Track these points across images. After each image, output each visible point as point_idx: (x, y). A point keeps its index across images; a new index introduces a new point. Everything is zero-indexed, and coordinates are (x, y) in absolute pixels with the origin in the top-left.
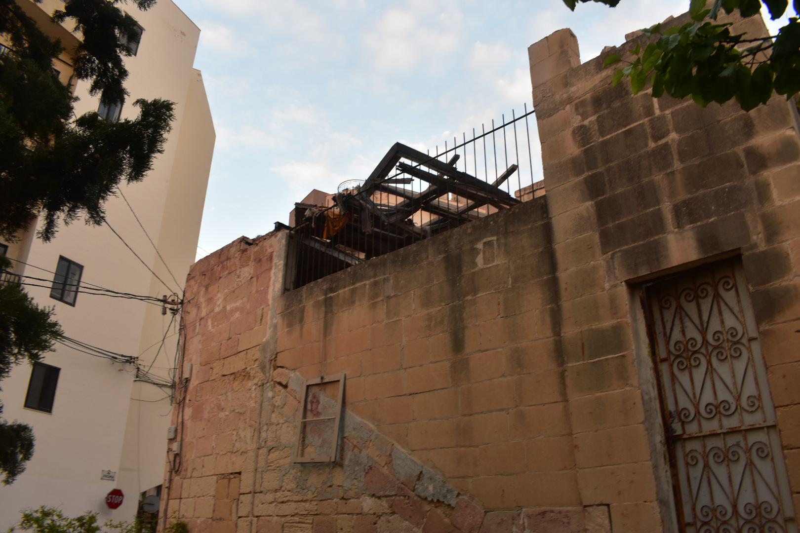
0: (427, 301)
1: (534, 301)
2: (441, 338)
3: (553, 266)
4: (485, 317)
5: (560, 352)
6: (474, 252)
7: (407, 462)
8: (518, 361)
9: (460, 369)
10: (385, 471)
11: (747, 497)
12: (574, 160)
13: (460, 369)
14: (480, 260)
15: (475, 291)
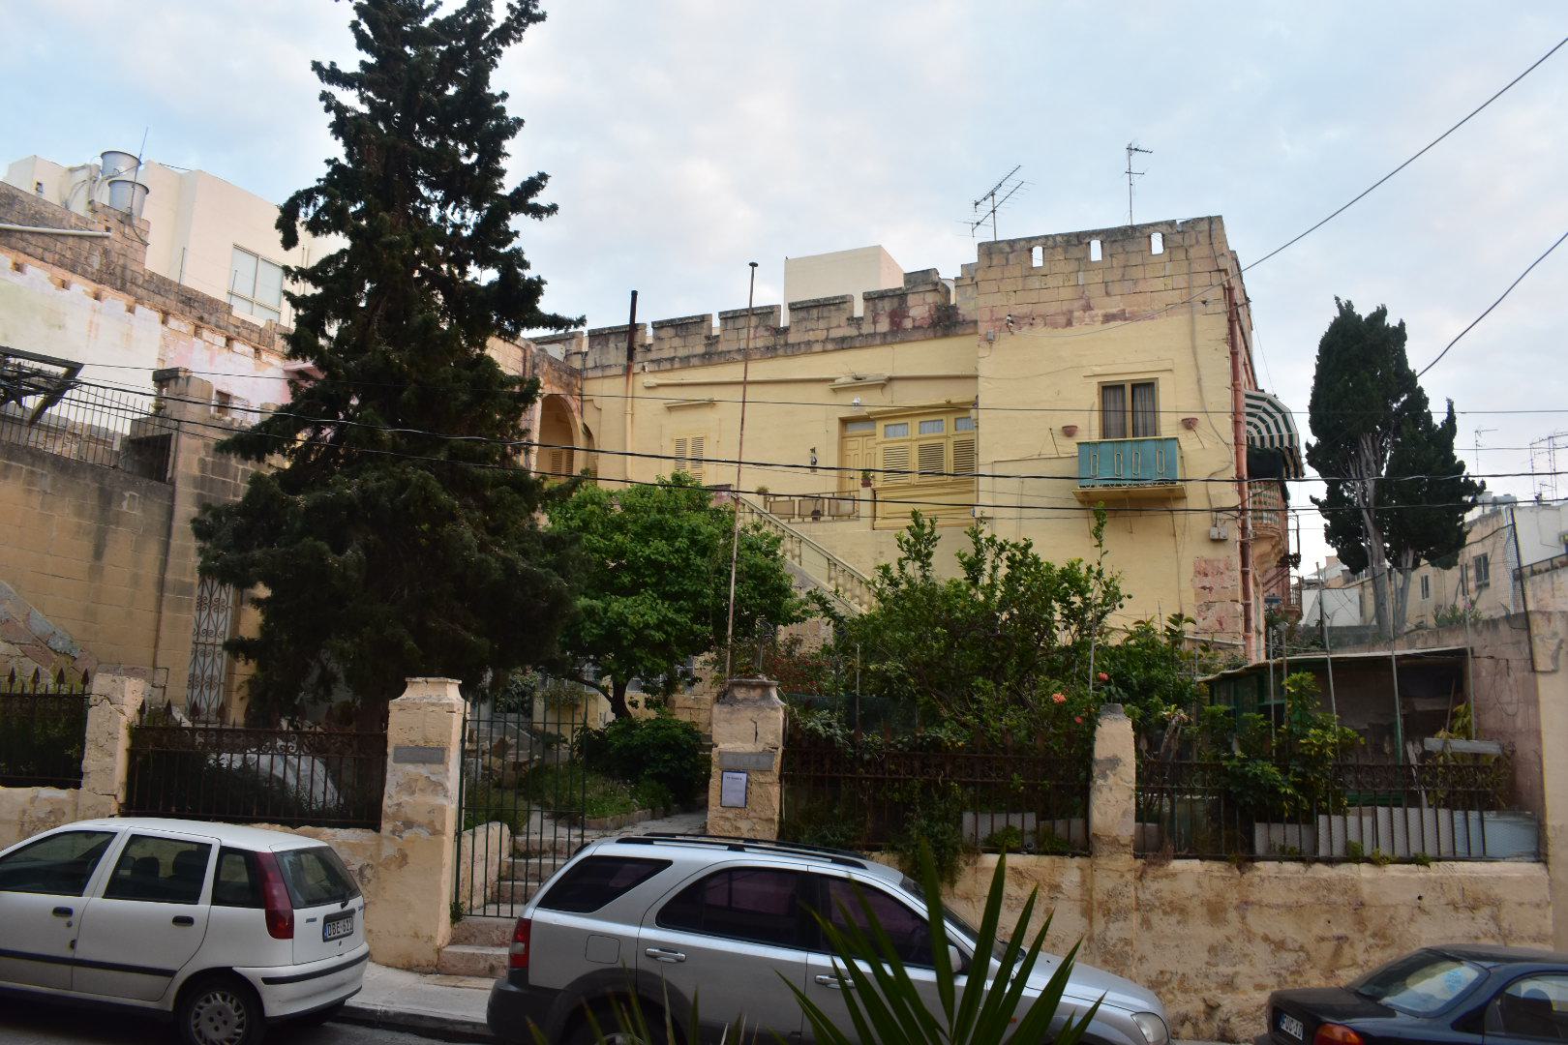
0: (80, 512)
1: (153, 550)
2: (86, 545)
3: (169, 534)
4: (121, 547)
5: (161, 585)
6: (123, 498)
7: (41, 624)
8: (135, 580)
9: (96, 571)
10: (21, 625)
11: (208, 673)
12: (195, 478)
13: (96, 571)
14: (125, 504)
15: (118, 524)
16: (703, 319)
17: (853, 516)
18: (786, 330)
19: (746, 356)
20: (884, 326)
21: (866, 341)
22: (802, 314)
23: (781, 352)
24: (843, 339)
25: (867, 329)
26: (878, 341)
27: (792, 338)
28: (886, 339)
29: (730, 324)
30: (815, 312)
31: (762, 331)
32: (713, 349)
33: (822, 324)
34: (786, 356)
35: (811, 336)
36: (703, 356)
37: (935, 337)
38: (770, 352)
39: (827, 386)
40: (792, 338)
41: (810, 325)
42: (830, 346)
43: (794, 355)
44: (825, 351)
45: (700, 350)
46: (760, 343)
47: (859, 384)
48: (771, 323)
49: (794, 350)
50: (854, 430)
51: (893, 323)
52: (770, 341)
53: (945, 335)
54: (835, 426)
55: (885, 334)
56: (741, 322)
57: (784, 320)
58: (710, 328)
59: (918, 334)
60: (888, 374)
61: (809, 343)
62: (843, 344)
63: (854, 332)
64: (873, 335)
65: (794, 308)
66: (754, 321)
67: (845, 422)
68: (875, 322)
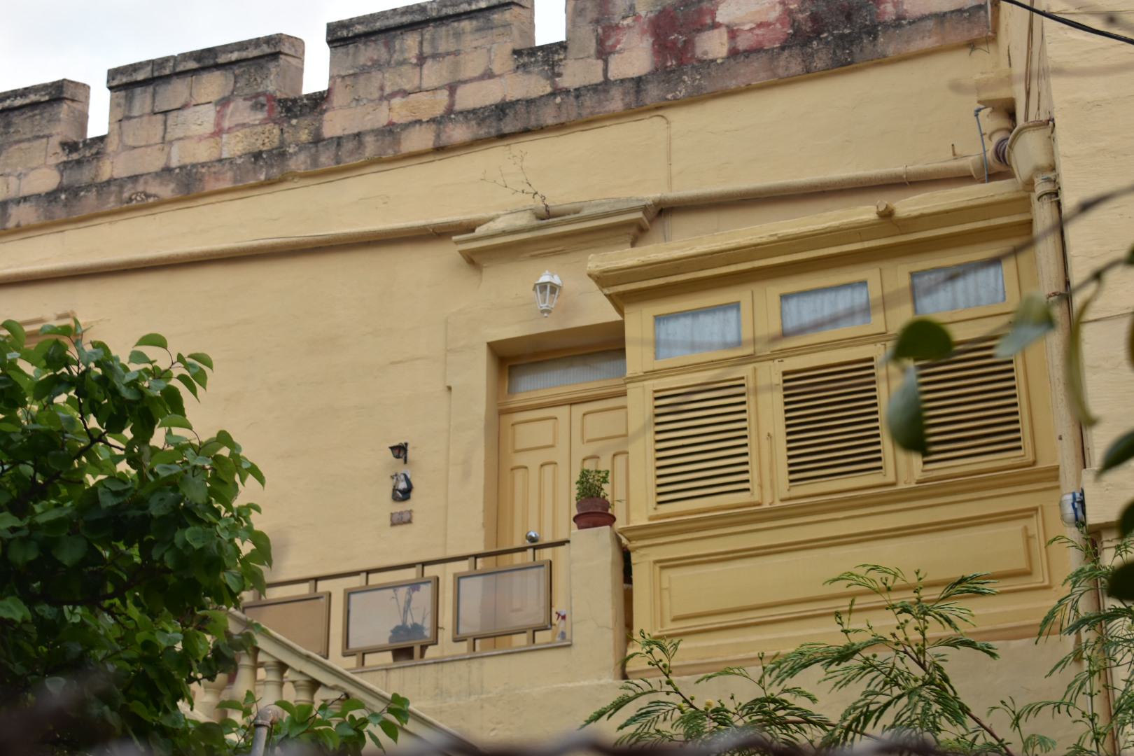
16: (59, 95)
17: (547, 632)
18: (319, 101)
19: (189, 185)
20: (635, 57)
21: (576, 110)
22: (368, 53)
23: (299, 162)
24: (502, 109)
25: (576, 74)
26: (616, 102)
27: (335, 124)
28: (639, 98)
29: (142, 101)
30: (410, 44)
31: (241, 112)
32: (85, 175)
33: (433, 74)
34: (317, 174)
35: (398, 111)
36: (52, 196)
37: (809, 74)
38: (266, 168)
39: (449, 252)
40: (335, 124)
41: (392, 80)
42: (458, 133)
43: (341, 170)
44: (440, 150)
45: (45, 179)
46: (234, 146)
47: (554, 232)
48: (272, 84)
49: (343, 157)
50: (537, 386)
51: (662, 47)
52: (269, 137)
53: (843, 64)
54: (476, 373)
55: (639, 82)
56: (176, 92)
57: (316, 73)
58: (82, 121)
59: (753, 71)
60: (652, 193)
61: (390, 131)
62: (503, 124)
63: (533, 85)
64: (605, 86)
65: (342, 36)
66: (213, 85)
67: (511, 360)
68: (603, 53)
